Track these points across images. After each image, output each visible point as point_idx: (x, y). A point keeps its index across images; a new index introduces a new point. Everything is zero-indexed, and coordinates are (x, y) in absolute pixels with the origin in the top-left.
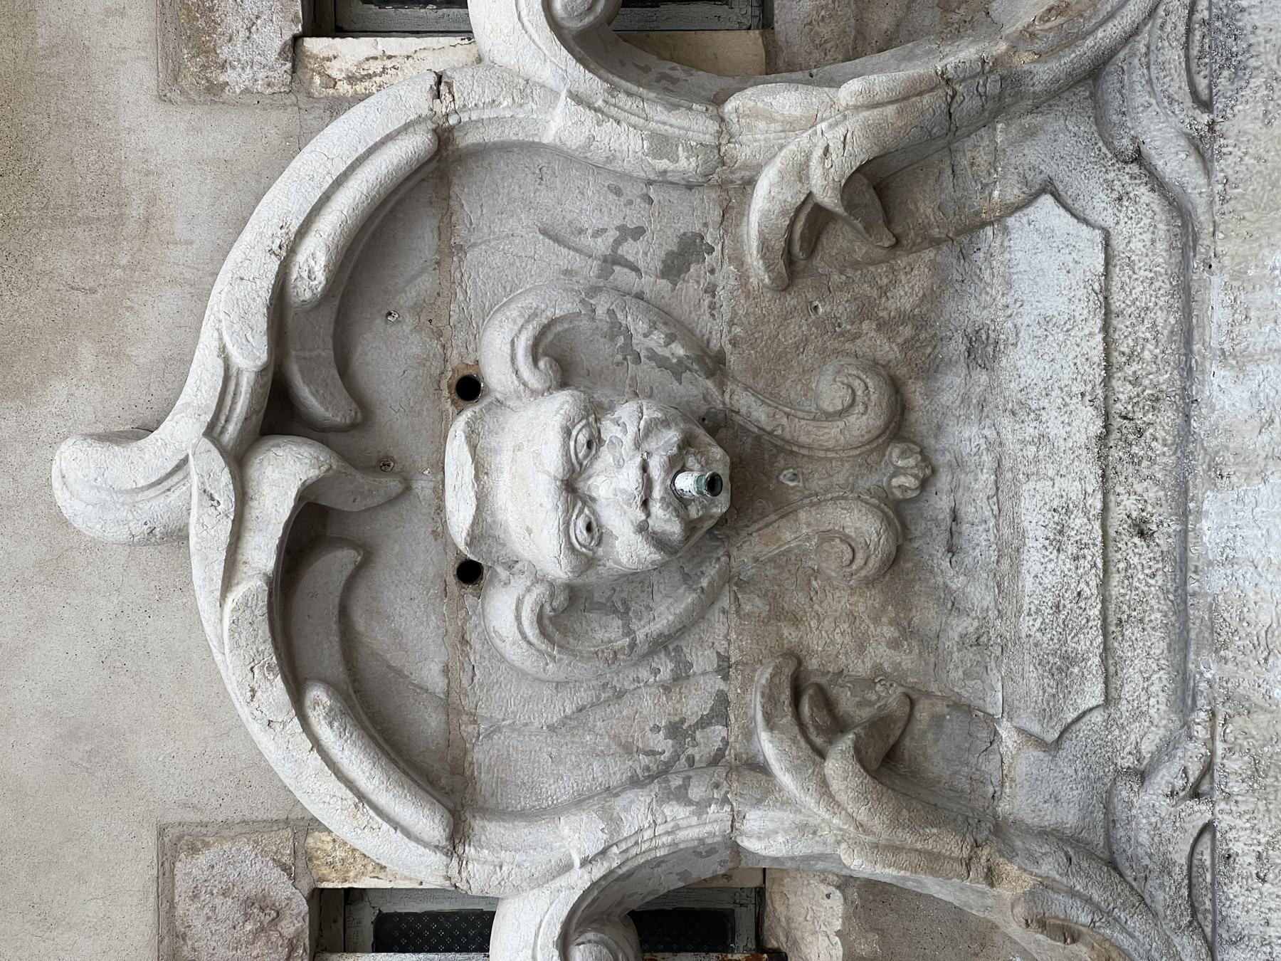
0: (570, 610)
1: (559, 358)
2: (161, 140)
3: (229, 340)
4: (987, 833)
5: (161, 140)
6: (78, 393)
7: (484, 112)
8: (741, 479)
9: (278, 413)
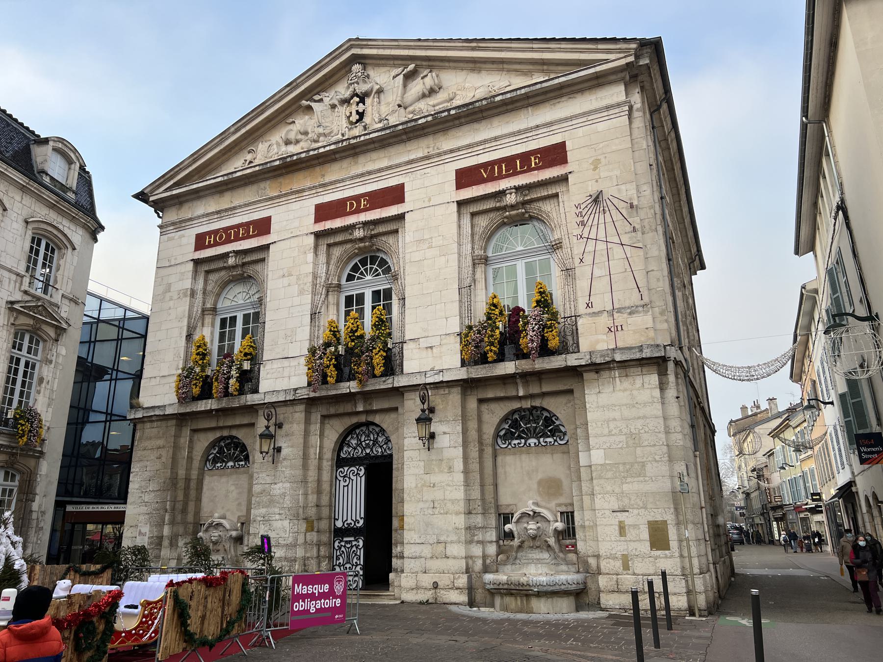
0: (525, 528)
1: (539, 528)
2: (552, 505)
3: (538, 510)
4: (517, 552)
5: (552, 505)
6: (539, 499)
7: (552, 523)
8: (534, 538)
9: (535, 513)
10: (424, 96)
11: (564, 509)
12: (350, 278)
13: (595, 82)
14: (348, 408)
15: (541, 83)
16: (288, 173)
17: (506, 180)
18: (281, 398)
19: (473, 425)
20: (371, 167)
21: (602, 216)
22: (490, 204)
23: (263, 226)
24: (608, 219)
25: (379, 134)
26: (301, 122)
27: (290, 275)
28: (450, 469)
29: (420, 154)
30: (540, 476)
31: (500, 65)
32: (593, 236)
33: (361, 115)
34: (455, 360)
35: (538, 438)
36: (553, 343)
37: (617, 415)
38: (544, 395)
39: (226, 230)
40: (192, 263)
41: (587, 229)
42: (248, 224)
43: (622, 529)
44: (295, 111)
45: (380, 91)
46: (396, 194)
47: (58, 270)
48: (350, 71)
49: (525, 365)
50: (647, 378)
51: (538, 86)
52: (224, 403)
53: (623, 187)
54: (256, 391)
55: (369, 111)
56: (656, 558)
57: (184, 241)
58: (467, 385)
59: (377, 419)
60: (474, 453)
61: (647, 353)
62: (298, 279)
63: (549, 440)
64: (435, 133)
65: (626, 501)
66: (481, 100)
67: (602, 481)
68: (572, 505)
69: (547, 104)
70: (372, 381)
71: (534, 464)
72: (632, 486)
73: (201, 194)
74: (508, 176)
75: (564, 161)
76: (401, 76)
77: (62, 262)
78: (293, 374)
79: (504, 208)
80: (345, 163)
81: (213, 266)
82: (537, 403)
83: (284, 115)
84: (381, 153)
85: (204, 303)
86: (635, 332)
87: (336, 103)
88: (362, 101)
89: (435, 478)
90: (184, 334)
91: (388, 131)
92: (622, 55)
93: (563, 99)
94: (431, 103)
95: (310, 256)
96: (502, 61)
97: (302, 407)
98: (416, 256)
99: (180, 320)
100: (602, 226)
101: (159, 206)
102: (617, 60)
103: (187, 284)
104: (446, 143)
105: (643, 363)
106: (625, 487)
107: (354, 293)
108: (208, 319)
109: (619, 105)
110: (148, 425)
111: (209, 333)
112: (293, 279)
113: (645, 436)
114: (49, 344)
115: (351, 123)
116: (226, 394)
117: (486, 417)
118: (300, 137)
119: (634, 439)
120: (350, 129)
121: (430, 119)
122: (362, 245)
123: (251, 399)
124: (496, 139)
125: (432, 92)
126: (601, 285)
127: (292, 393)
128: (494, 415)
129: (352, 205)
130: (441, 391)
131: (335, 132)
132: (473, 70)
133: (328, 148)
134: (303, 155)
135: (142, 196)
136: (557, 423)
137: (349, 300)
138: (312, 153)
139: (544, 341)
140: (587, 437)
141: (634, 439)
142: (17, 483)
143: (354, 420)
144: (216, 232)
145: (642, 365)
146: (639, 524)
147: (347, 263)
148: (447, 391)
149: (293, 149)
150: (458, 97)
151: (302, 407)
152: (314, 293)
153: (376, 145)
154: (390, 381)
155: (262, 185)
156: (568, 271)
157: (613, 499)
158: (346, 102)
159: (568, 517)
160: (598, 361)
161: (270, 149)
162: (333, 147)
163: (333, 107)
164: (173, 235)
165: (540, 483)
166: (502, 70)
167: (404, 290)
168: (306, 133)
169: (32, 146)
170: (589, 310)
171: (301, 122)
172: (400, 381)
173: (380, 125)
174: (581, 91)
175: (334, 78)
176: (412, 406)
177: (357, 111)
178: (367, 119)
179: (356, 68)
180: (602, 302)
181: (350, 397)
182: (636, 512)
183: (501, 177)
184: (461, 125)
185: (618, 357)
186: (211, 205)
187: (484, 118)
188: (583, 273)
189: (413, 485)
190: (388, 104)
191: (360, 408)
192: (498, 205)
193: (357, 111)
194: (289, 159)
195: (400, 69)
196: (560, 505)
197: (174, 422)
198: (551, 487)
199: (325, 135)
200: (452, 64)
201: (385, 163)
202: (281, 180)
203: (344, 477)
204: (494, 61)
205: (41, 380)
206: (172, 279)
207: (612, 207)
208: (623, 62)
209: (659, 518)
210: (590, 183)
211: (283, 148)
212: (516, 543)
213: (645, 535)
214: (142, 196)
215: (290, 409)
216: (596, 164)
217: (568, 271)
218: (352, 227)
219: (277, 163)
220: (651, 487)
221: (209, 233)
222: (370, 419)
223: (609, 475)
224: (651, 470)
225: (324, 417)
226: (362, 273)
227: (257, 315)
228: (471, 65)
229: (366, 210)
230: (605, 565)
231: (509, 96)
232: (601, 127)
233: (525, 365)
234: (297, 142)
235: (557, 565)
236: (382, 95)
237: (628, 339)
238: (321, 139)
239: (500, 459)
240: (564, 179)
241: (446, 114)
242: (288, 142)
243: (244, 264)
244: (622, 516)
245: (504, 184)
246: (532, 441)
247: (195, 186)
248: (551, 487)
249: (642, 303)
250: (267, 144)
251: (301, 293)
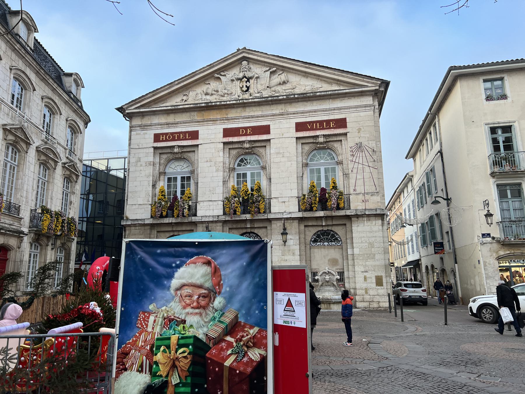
2: (334, 269)
3: (330, 271)
5: (334, 269)
8: (328, 282)
10: (280, 84)
11: (339, 271)
12: (239, 165)
13: (360, 94)
14: (243, 225)
15: (338, 90)
16: (207, 110)
17: (319, 131)
18: (211, 219)
19: (302, 236)
20: (252, 114)
21: (361, 153)
22: (311, 140)
23: (194, 135)
24: (364, 155)
25: (259, 100)
26: (214, 84)
27: (211, 161)
28: (294, 254)
29: (277, 112)
30: (329, 257)
31: (318, 77)
32: (357, 161)
33: (248, 88)
34: (296, 209)
35: (328, 242)
36: (342, 205)
37: (365, 235)
38: (333, 225)
39: (172, 134)
40: (153, 148)
41: (355, 158)
42: (185, 133)
43: (365, 278)
44: (210, 78)
45: (257, 78)
46: (266, 130)
47: (75, 145)
48: (241, 63)
49: (328, 213)
50: (377, 222)
51: (337, 92)
52: (179, 220)
53: (370, 142)
54: (195, 215)
55: (252, 86)
56: (378, 289)
57: (147, 136)
58: (301, 220)
59: (256, 231)
60: (303, 248)
61: (378, 212)
62: (215, 164)
63: (333, 243)
64: (285, 103)
65: (367, 268)
66: (310, 93)
67: (358, 261)
68: (343, 269)
69: (338, 99)
70: (259, 215)
71: (327, 252)
72: (370, 263)
73: (156, 113)
74: (320, 129)
75: (345, 127)
76: (269, 73)
77: (76, 140)
78: (215, 208)
79: (317, 143)
80: (239, 110)
81: (164, 151)
82: (330, 228)
83: (204, 79)
84: (258, 108)
85: (159, 169)
86: (373, 203)
87: (234, 79)
88: (248, 81)
89: (286, 258)
90: (151, 184)
91: (264, 99)
92: (374, 85)
93: (346, 98)
94: (284, 88)
95: (221, 154)
96: (319, 76)
97: (221, 224)
98: (277, 160)
99: (148, 176)
100: (361, 158)
101: (129, 116)
102: (372, 87)
103: (151, 159)
104: (291, 109)
105: (376, 215)
106: (367, 263)
107: (242, 172)
108: (162, 177)
109: (370, 106)
110: (133, 228)
111: (162, 184)
112: (212, 163)
113: (375, 244)
114: (74, 183)
115: (243, 91)
116: (184, 216)
117: (307, 233)
118: (214, 92)
119: (371, 245)
120: (243, 94)
121: (285, 97)
122: (247, 151)
123: (194, 219)
124: (315, 111)
125: (284, 83)
126: (360, 182)
127: (217, 217)
128: (311, 233)
129: (243, 131)
130: (289, 221)
131: (234, 93)
132: (304, 76)
133: (231, 102)
134: (218, 103)
135: (121, 110)
136: (337, 236)
137: (239, 175)
138: (223, 103)
139: (338, 204)
140: (352, 243)
141: (371, 245)
142: (63, 255)
143: (244, 231)
144: (166, 134)
145: (375, 216)
146: (372, 276)
147: (237, 158)
148: (292, 221)
149: (209, 98)
150: (297, 88)
151: (221, 224)
152: (224, 171)
153: (256, 104)
154: (266, 215)
155: (193, 113)
156: (346, 175)
157: (362, 267)
158: (241, 79)
159: (341, 274)
160: (359, 214)
161: (197, 96)
162: (234, 102)
163: (232, 80)
164: (140, 132)
165: (329, 260)
166: (318, 79)
167: (270, 174)
168: (217, 91)
169: (62, 76)
170: (355, 192)
171: (213, 85)
172: (271, 216)
173: (258, 95)
174: (354, 96)
175: (232, 65)
176: (277, 227)
177: (246, 86)
178: (251, 90)
179: (245, 63)
180: (360, 189)
181: (245, 221)
182: (371, 272)
183: (316, 129)
184: (298, 102)
185: (367, 213)
186: (162, 119)
187: (309, 100)
188: (352, 176)
189: (277, 260)
190: (262, 85)
191: (249, 226)
192: (314, 141)
193: (246, 86)
194: (210, 104)
195: (268, 68)
196: (337, 269)
197: (149, 227)
198: (334, 262)
199: (228, 94)
200: (294, 71)
201: (260, 113)
202: (203, 112)
204: (315, 75)
205: (71, 203)
206: (141, 155)
207: (365, 150)
208: (374, 88)
209: (380, 275)
210: (356, 138)
211: (204, 97)
212: (320, 283)
213: (374, 281)
214: (121, 110)
215: (214, 225)
216: (359, 130)
217: (346, 175)
218: (243, 142)
219: (203, 105)
220: (377, 263)
221: (163, 134)
222: (252, 231)
223: (361, 258)
224: (377, 257)
225: (229, 229)
226: (245, 163)
227: (189, 178)
228: (304, 74)
229: (250, 135)
230: (358, 292)
231: (323, 93)
232: (362, 114)
233: (328, 213)
234: (212, 94)
235: (337, 292)
236: (258, 80)
237: (371, 205)
238: (226, 95)
239: (312, 250)
240: (345, 134)
241: (293, 96)
242: (207, 94)
243: (182, 152)
244: (365, 274)
245: (318, 133)
246: (326, 244)
247: (154, 109)
248: (334, 262)
249: (376, 191)
250: (195, 93)
251: (217, 171)
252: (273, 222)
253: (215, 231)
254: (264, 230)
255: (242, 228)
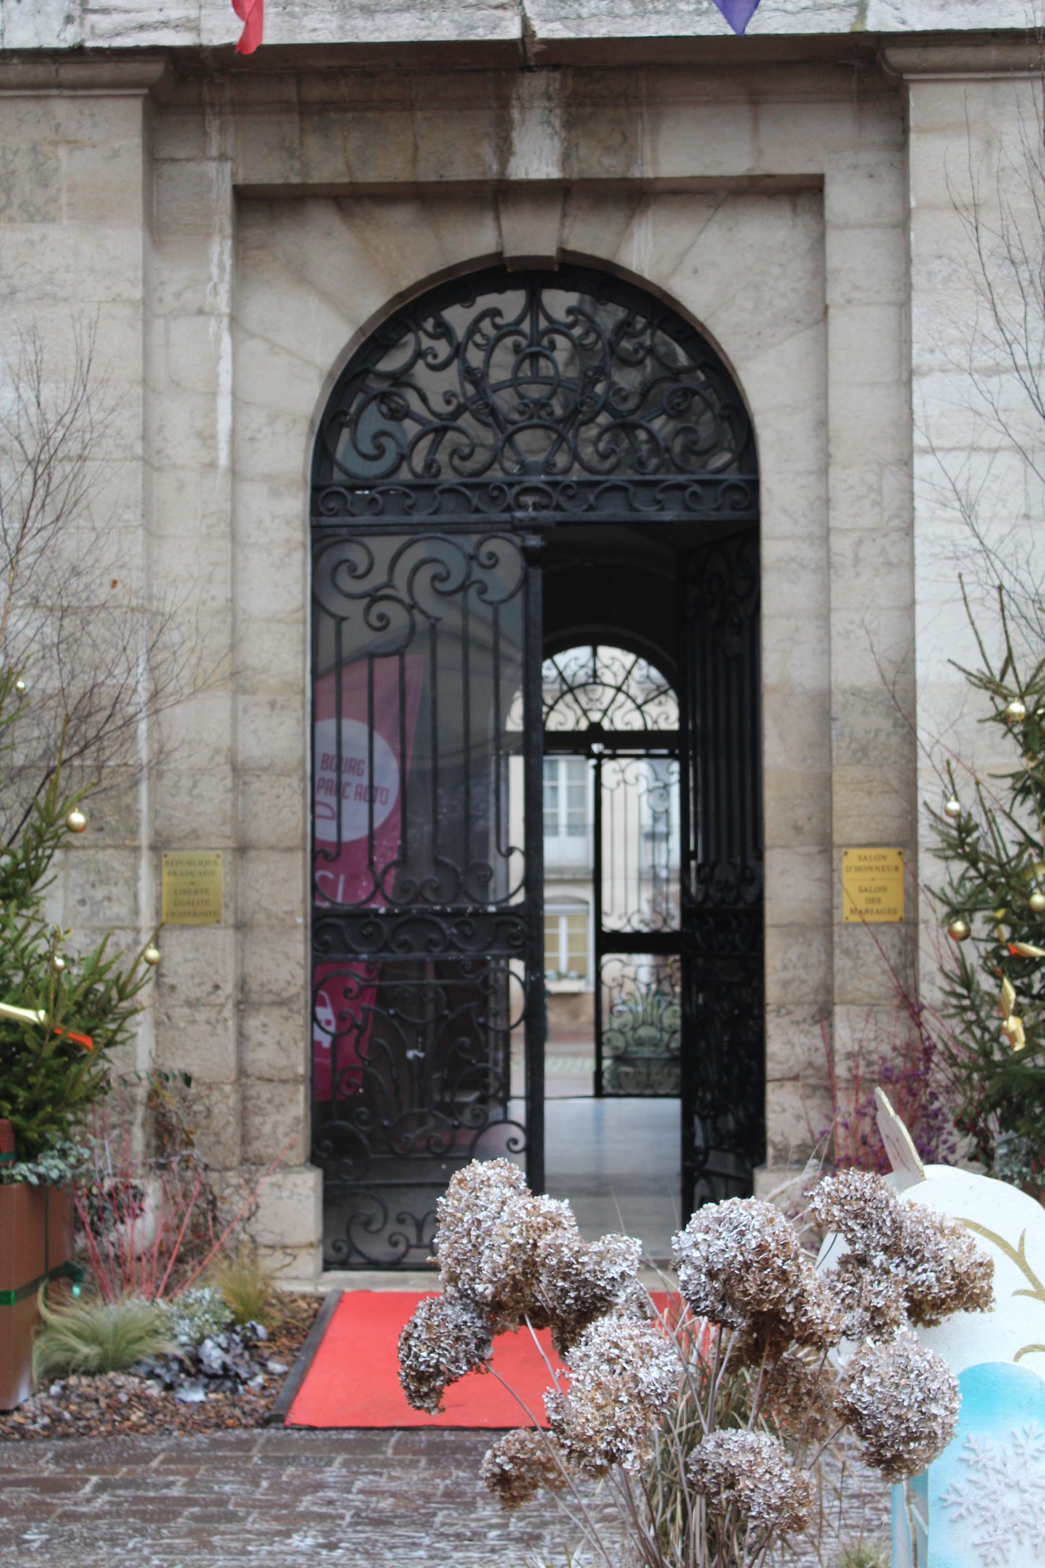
14: (453, 153)
59: (645, 249)
143: (475, 239)
191: (537, 157)
203: (374, 597)
222: (589, 236)
225: (249, 201)
252: (926, 101)
253: (34, 214)
254: (765, 235)
255: (433, 198)
